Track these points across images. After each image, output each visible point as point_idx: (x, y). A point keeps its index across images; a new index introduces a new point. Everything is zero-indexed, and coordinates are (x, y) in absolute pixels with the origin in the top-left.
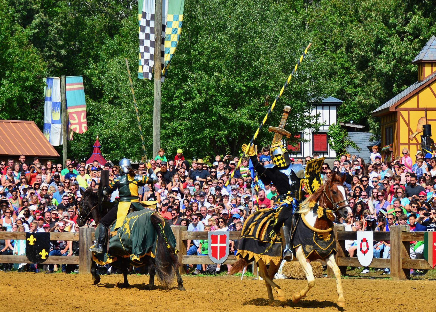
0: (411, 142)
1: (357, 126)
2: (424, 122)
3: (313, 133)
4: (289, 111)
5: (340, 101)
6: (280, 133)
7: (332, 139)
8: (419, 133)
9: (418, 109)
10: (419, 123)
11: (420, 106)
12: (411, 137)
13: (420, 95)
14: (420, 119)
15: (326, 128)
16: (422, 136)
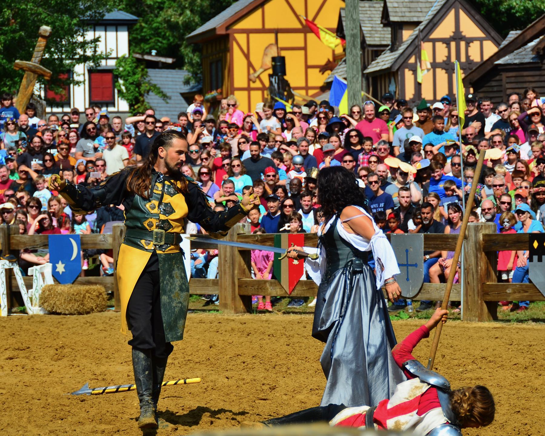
0: (252, 85)
1: (163, 60)
2: (274, 52)
3: (90, 71)
4: (47, 34)
5: (134, 17)
6: (34, 72)
7: (121, 81)
8: (265, 70)
9: (263, 31)
10: (265, 54)
11: (267, 26)
12: (252, 77)
13: (267, 7)
14: (267, 48)
15: (112, 63)
16: (270, 76)
